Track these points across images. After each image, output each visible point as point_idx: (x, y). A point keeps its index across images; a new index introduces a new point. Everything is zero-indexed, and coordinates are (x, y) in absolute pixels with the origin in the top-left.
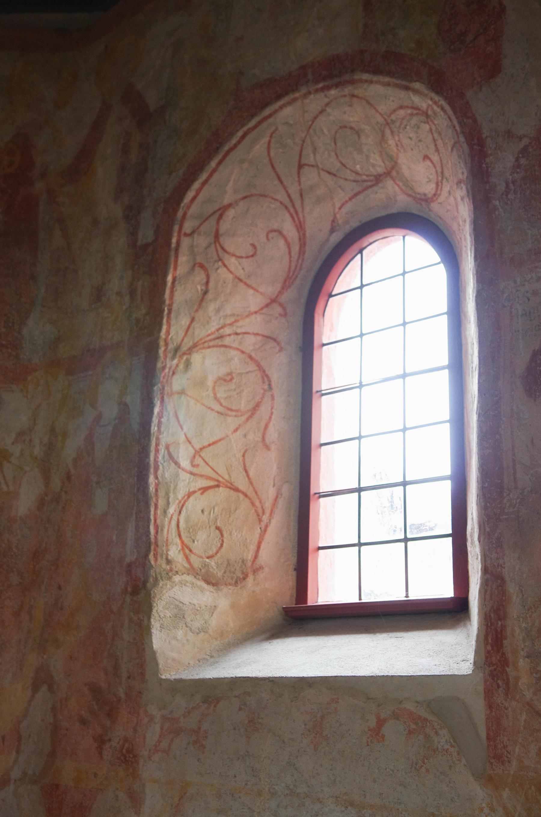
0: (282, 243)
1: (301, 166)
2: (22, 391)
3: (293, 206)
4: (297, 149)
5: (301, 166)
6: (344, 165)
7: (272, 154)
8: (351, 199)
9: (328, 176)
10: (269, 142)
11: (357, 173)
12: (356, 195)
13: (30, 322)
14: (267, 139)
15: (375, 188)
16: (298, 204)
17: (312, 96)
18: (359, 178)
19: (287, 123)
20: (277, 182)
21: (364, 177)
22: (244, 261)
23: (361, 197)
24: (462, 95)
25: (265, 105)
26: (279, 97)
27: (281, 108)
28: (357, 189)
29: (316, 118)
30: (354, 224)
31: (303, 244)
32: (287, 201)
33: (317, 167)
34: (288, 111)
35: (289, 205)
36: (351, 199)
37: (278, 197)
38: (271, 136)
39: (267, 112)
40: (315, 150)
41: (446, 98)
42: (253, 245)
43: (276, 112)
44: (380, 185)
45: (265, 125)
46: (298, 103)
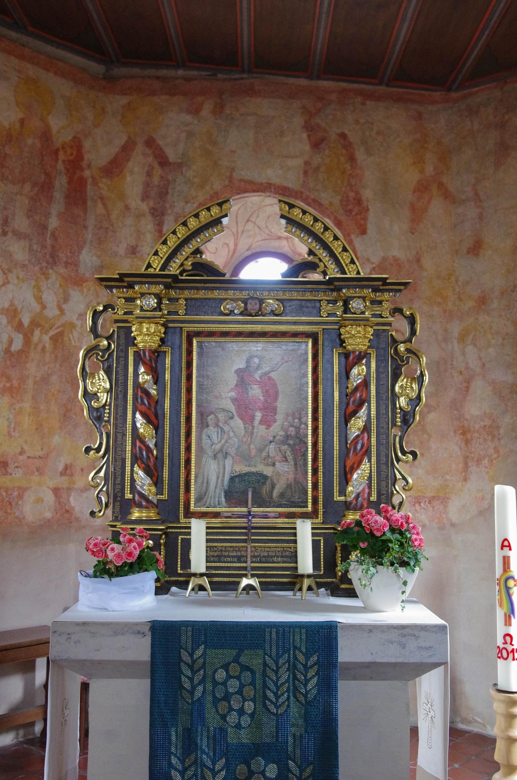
0: (227, 250)
1: (248, 221)
2: (80, 291)
3: (237, 235)
4: (250, 213)
5: (248, 221)
6: (267, 227)
7: (239, 212)
8: (262, 240)
9: (257, 228)
10: (240, 207)
11: (271, 232)
12: (266, 239)
13: (84, 252)
14: (240, 205)
15: (276, 241)
16: (239, 235)
17: (270, 198)
18: (270, 234)
19: (252, 202)
20: (235, 224)
21: (273, 235)
22: (212, 255)
23: (267, 241)
24: (349, 235)
25: (245, 192)
26: (254, 191)
27: (253, 196)
28: (267, 237)
29: (266, 206)
30: (258, 250)
31: (234, 252)
32: (235, 232)
33: (255, 223)
34: (255, 198)
35: (236, 235)
36: (262, 240)
37: (233, 230)
38: (243, 205)
39: (246, 195)
40: (258, 217)
41: (342, 233)
42: (216, 248)
43: (250, 196)
44: (279, 240)
45: (242, 199)
46: (262, 198)
